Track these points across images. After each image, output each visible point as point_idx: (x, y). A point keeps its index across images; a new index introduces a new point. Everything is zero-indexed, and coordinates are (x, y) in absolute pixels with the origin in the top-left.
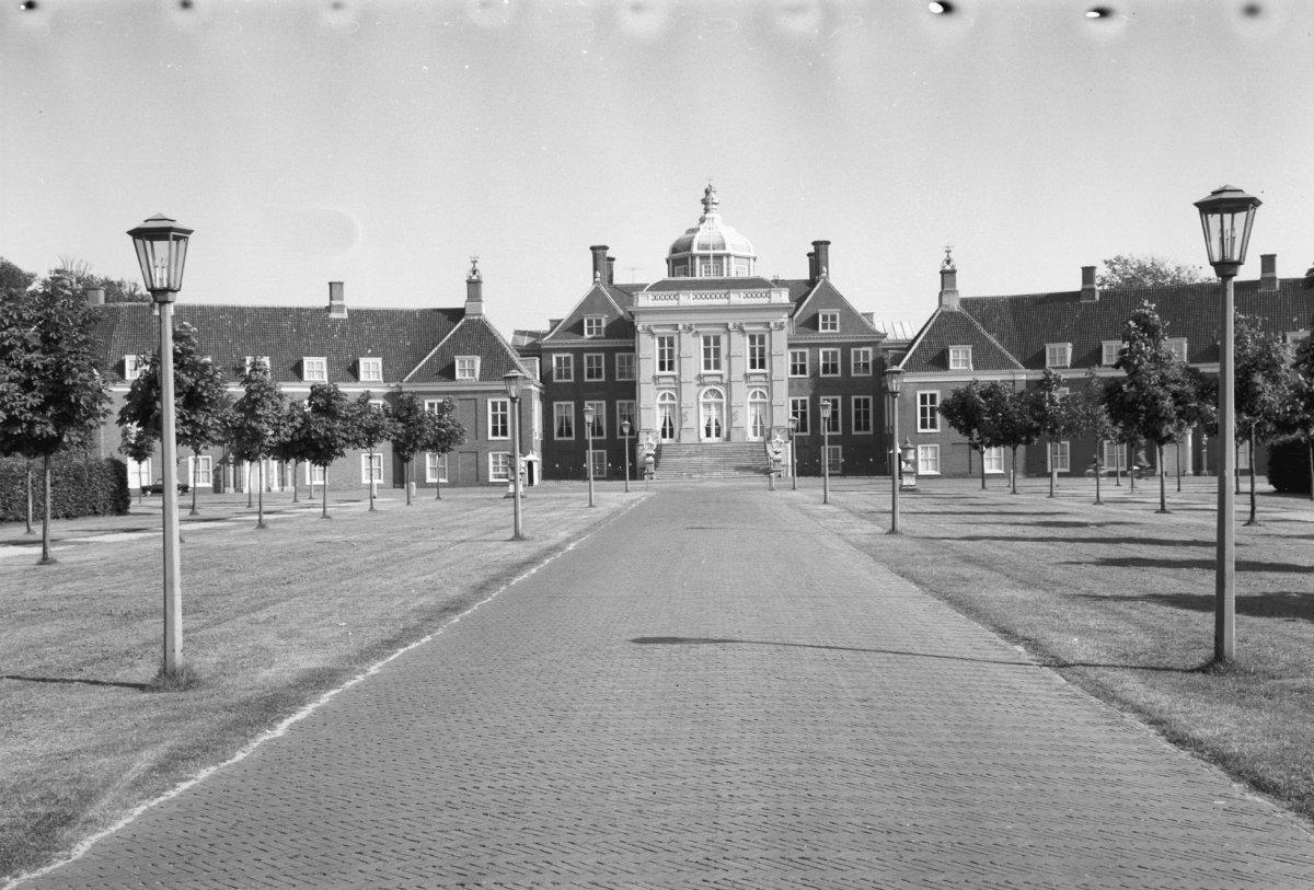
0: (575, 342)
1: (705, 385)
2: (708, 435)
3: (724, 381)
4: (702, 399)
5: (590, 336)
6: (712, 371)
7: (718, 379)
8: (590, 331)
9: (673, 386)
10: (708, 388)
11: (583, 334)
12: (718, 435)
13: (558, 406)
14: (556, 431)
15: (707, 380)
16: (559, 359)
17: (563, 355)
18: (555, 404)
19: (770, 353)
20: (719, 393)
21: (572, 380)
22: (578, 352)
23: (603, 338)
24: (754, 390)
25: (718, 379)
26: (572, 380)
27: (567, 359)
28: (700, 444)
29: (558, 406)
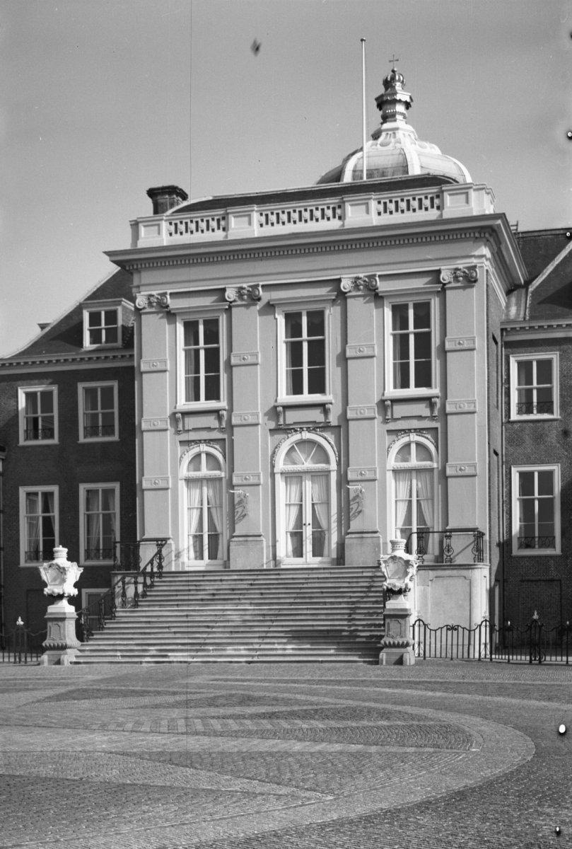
0: (62, 361)
1: (285, 430)
2: (298, 552)
3: (333, 419)
4: (281, 465)
5: (95, 346)
6: (306, 397)
7: (317, 416)
8: (95, 337)
9: (216, 435)
10: (296, 437)
11: (80, 343)
12: (317, 551)
13: (28, 494)
14: (24, 547)
15: (292, 417)
16: (30, 397)
17: (38, 389)
18: (22, 492)
19: (443, 344)
20: (320, 447)
21: (55, 441)
22: (68, 381)
23: (117, 349)
24: (405, 440)
25: (317, 416)
26: (55, 441)
27: (47, 396)
28: (277, 570)
29: (28, 494)
